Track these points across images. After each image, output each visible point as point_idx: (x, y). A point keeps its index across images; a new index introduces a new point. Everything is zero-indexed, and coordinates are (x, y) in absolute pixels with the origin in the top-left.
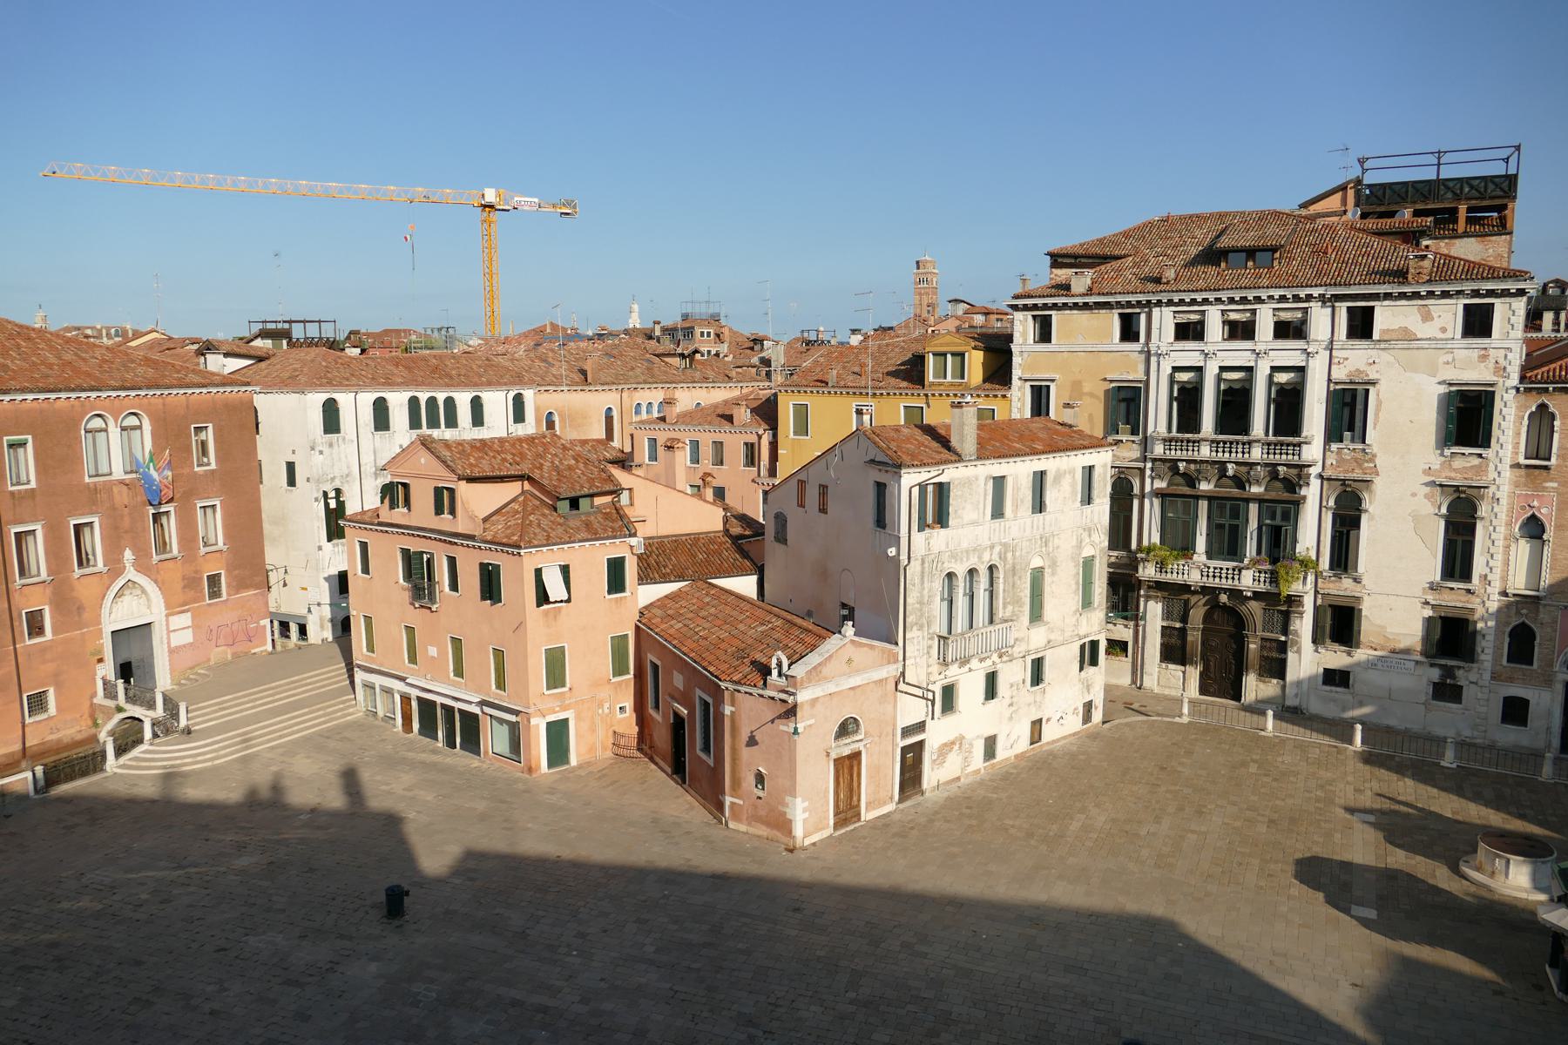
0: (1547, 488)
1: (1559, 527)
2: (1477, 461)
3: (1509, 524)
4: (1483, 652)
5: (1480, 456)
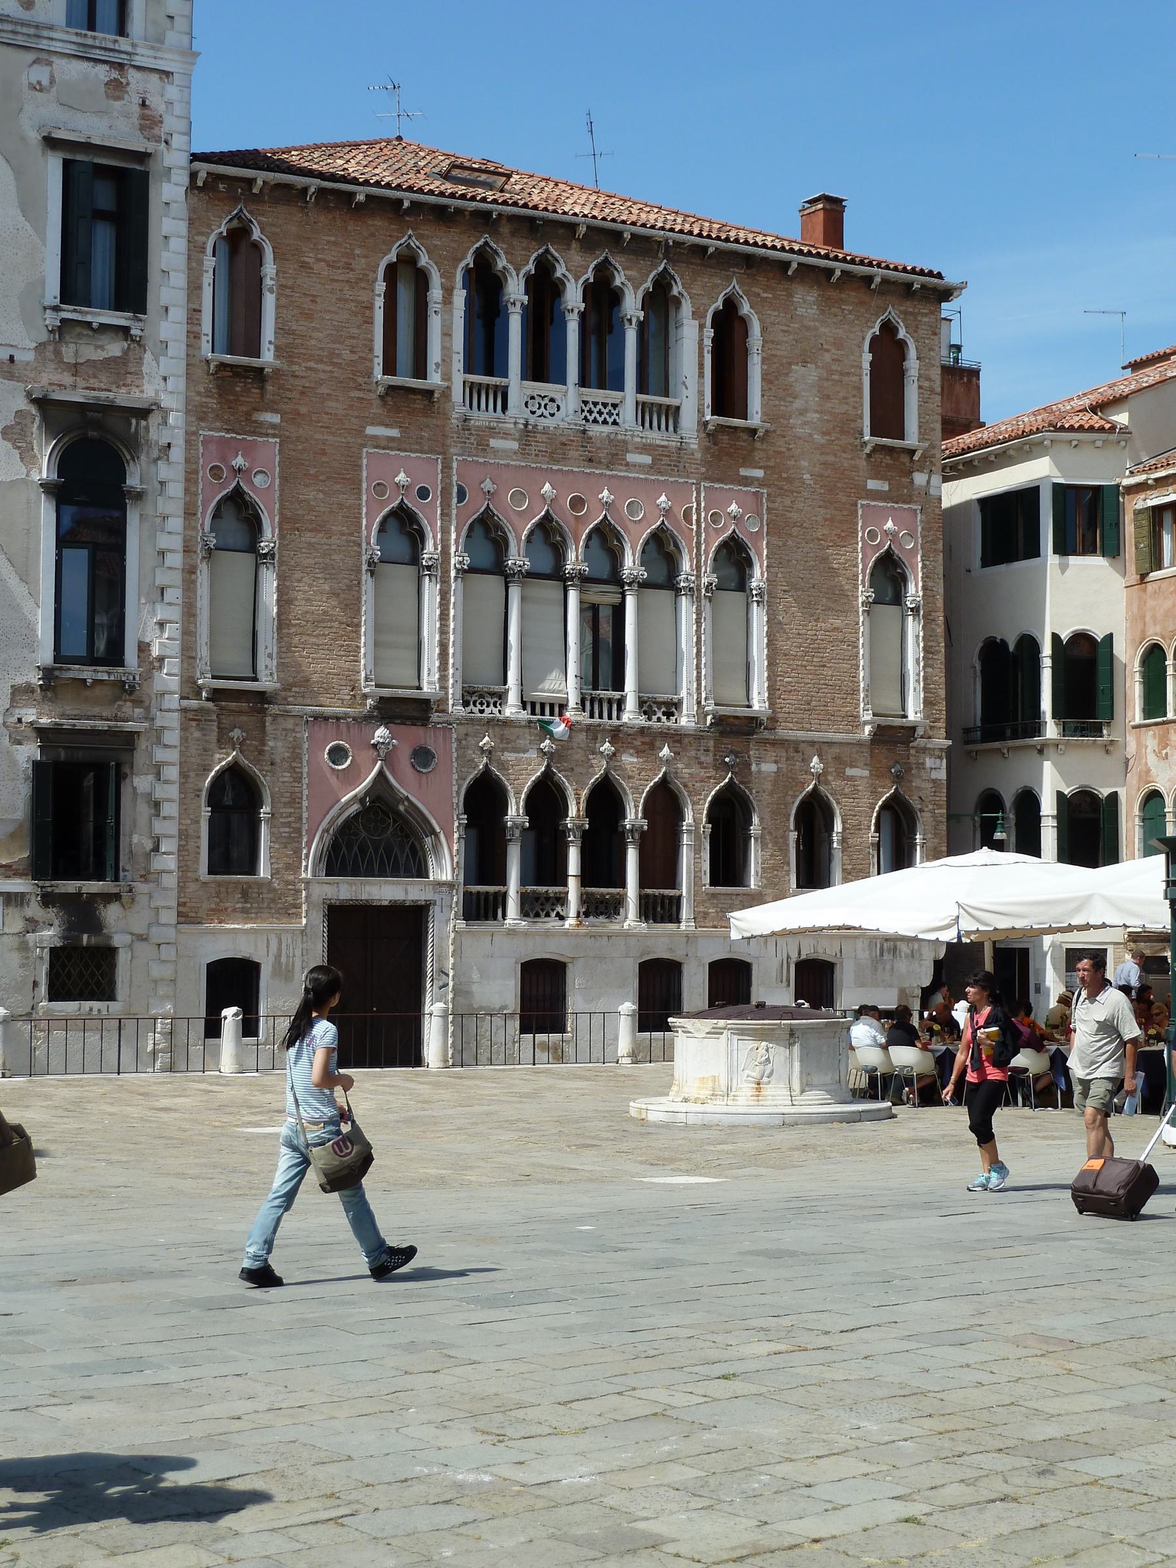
1: (288, 524)
2: (115, 348)
3: (189, 513)
4: (156, 849)
5: (125, 330)
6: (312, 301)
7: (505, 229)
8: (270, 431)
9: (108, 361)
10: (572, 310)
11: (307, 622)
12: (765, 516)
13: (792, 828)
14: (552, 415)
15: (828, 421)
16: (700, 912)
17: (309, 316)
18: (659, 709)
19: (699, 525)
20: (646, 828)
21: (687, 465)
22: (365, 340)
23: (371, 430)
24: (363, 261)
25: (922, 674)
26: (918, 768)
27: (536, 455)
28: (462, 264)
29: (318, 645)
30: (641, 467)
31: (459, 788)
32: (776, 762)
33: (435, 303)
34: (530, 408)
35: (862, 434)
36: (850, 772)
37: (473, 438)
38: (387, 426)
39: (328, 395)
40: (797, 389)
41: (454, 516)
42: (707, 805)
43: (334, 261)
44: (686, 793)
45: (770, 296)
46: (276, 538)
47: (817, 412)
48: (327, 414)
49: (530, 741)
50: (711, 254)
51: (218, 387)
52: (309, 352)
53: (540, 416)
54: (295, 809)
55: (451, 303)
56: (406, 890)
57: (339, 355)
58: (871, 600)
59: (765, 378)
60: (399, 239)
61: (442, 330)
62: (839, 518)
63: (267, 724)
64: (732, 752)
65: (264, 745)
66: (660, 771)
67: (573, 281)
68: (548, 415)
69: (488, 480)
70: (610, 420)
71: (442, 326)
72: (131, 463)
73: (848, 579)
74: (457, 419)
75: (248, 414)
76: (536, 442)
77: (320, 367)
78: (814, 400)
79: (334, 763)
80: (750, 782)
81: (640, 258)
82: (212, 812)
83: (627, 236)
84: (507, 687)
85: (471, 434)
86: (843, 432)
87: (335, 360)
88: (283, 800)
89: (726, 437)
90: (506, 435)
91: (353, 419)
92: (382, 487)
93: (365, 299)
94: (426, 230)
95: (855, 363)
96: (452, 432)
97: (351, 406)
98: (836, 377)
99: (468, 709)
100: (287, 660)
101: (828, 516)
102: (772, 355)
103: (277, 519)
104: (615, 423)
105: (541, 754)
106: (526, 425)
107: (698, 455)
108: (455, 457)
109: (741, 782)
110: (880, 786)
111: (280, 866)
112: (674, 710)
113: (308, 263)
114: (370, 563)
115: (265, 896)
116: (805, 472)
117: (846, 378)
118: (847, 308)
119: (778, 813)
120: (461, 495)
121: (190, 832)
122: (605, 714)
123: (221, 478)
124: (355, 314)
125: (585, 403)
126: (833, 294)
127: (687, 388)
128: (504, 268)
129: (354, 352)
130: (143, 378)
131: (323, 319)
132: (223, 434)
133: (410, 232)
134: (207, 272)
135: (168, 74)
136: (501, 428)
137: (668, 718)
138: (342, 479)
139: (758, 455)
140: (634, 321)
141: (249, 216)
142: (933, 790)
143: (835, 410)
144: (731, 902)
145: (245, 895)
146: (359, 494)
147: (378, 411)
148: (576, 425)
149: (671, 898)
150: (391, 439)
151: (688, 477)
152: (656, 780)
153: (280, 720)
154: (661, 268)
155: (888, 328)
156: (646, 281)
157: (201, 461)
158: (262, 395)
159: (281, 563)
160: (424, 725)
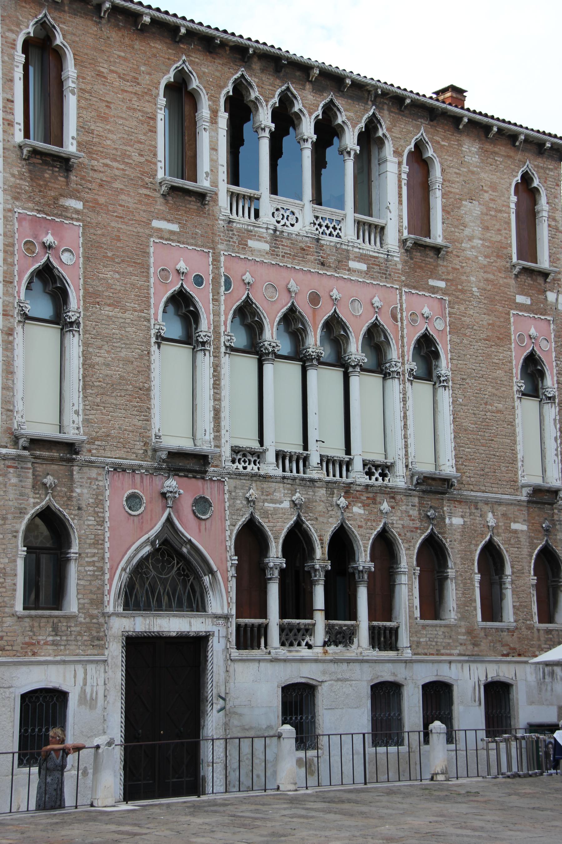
0: (66, 209)
6: (107, 106)
7: (257, 65)
8: (75, 216)
10: (307, 140)
11: (108, 384)
12: (448, 319)
13: (476, 571)
14: (292, 225)
15: (489, 247)
16: (413, 641)
17: (104, 119)
18: (376, 470)
19: (402, 323)
20: (373, 569)
22: (150, 146)
23: (156, 224)
24: (147, 77)
28: (224, 92)
29: (116, 405)
30: (360, 272)
31: (231, 533)
32: (462, 517)
33: (204, 121)
34: (276, 218)
35: (511, 258)
36: (514, 526)
37: (235, 238)
38: (169, 221)
39: (121, 189)
40: (467, 220)
41: (222, 302)
42: (416, 551)
43: (124, 74)
44: (400, 541)
45: (447, 144)
46: (81, 310)
47: (480, 239)
48: (121, 205)
49: (284, 494)
50: (408, 104)
51: (30, 171)
52: (105, 150)
53: (284, 225)
54: (98, 549)
55: (216, 123)
56: (190, 623)
57: (129, 157)
58: (522, 389)
59: (444, 210)
60: (175, 62)
61: (210, 145)
62: (498, 324)
63: (75, 473)
64: (431, 507)
65: (72, 491)
67: (307, 116)
68: (289, 225)
69: (248, 273)
70: (335, 233)
71: (210, 141)
73: (506, 372)
74: (223, 220)
75: (56, 199)
76: (283, 245)
77: (115, 164)
78: (478, 231)
79: (130, 508)
80: (444, 533)
81: (356, 103)
83: (348, 81)
84: (264, 448)
85: (233, 234)
86: (498, 256)
87: (126, 160)
88: (88, 541)
89: (419, 254)
90: (260, 238)
91: (142, 212)
93: (149, 111)
94: (197, 57)
95: (505, 203)
96: (219, 232)
97: (140, 202)
98: (493, 213)
99: (235, 466)
100: (91, 417)
101: (491, 322)
102: (449, 191)
103: (81, 292)
104: (338, 236)
105: (292, 505)
106: (275, 230)
107: (400, 266)
108: (222, 252)
109: (439, 533)
110: (535, 538)
111: (86, 601)
112: (387, 472)
113: (103, 73)
115: (73, 629)
116: (474, 286)
117: (499, 214)
118: (499, 159)
119: (466, 558)
121: (8, 569)
122: (331, 474)
123: (34, 252)
125: (317, 218)
126: (488, 147)
127: (390, 212)
128: (256, 98)
131: (116, 123)
132: (35, 214)
133: (184, 57)
134: (18, 67)
136: (256, 232)
137: (383, 480)
138: (134, 263)
139: (441, 270)
140: (352, 153)
141: (53, 22)
143: (492, 239)
144: (436, 632)
145: (56, 630)
146: (148, 277)
147: (161, 208)
148: (312, 233)
149: (391, 629)
150: (172, 232)
151: (393, 283)
152: (379, 529)
153: (85, 469)
154: (371, 113)
155: (526, 178)
156: (360, 122)
157: (17, 235)
158: (67, 185)
159: (85, 332)
160: (203, 478)
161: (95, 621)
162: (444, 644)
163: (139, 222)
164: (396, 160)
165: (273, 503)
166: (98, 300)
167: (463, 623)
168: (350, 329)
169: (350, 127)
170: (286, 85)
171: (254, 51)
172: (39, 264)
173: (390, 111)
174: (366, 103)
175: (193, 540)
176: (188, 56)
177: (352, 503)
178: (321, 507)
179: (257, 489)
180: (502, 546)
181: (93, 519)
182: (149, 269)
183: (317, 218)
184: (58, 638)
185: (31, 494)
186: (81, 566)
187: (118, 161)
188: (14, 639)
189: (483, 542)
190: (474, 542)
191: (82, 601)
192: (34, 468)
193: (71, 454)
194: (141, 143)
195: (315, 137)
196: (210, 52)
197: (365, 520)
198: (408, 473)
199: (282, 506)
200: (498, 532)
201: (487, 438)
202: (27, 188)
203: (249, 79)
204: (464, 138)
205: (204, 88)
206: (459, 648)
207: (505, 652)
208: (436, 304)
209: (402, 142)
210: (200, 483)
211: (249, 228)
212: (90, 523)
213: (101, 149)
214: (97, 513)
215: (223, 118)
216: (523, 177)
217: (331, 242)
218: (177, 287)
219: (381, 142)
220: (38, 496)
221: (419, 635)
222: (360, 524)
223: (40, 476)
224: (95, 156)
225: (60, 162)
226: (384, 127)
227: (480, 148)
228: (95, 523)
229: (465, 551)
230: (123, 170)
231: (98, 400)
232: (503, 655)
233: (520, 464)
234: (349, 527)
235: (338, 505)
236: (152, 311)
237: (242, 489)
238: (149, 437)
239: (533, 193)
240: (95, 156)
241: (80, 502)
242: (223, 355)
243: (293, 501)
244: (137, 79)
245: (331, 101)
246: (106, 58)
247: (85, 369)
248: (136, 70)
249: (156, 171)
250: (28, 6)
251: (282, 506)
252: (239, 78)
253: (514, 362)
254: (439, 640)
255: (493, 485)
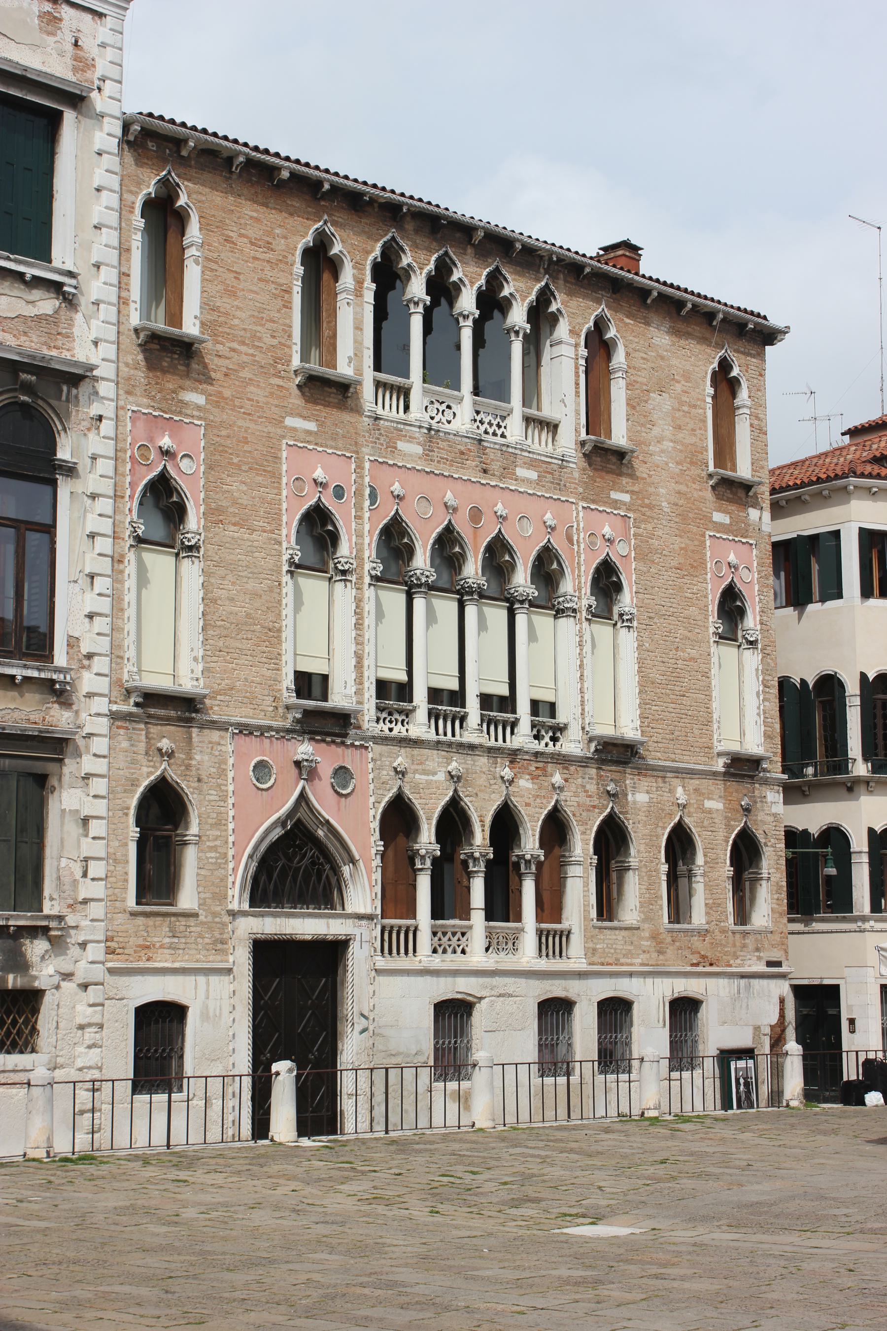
0: (186, 404)
1: (214, 515)
2: (47, 304)
4: (85, 875)
6: (235, 278)
7: (410, 226)
8: (195, 413)
9: (39, 318)
10: (468, 316)
11: (232, 623)
12: (633, 542)
13: (663, 860)
15: (681, 451)
17: (231, 293)
18: (547, 733)
19: (579, 546)
21: (568, 484)
22: (285, 325)
23: (290, 422)
24: (283, 241)
25: (762, 707)
26: (761, 801)
27: (438, 462)
28: (371, 258)
36: (708, 804)
37: (382, 438)
38: (305, 418)
39: (250, 379)
41: (366, 520)
42: (593, 835)
43: (256, 239)
44: (575, 823)
47: (672, 441)
48: (249, 399)
50: (588, 273)
51: (146, 359)
52: (233, 331)
53: (438, 422)
54: (221, 831)
55: (361, 296)
57: (260, 339)
58: (720, 631)
61: (354, 323)
62: (692, 548)
66: (552, 798)
67: (469, 287)
68: (445, 422)
69: (397, 483)
70: (499, 432)
71: (355, 318)
72: (62, 433)
73: (700, 609)
74: (369, 417)
76: (438, 448)
77: (243, 349)
78: (668, 432)
79: (258, 780)
80: (626, 813)
81: (526, 271)
82: (140, 833)
83: (518, 246)
84: (414, 704)
85: (380, 434)
86: (692, 463)
87: (256, 343)
88: (210, 821)
89: (599, 459)
90: (411, 439)
91: (273, 408)
92: (300, 482)
94: (340, 217)
95: (700, 397)
97: (272, 394)
98: (686, 408)
101: (683, 545)
102: (635, 381)
107: (576, 475)
108: (367, 457)
111: (208, 895)
113: (232, 237)
114: (291, 563)
115: (192, 929)
116: (663, 499)
119: (652, 845)
120: (373, 497)
123: (148, 459)
124: (275, 296)
126: (680, 326)
127: (566, 406)
128: (409, 265)
129: (274, 337)
130: (74, 340)
133: (326, 217)
135: (101, 15)
136: (407, 431)
137: (554, 746)
138: (264, 471)
141: (177, 180)
142: (774, 824)
143: (685, 441)
144: (614, 937)
146: (279, 488)
150: (309, 432)
152: (550, 808)
155: (725, 366)
161: (217, 920)
162: (624, 952)
163: (270, 420)
164: (573, 341)
165: (424, 774)
166: (221, 518)
167: (646, 926)
168: (518, 554)
169: (519, 300)
170: (444, 249)
171: (408, 209)
172: (155, 473)
173: (566, 281)
174: (538, 271)
175: (332, 821)
176: (329, 215)
177: (519, 775)
178: (482, 781)
179: (407, 757)
180: (693, 830)
181: (215, 793)
182: (280, 479)
183: (478, 413)
184: (176, 940)
185: (145, 762)
186: (202, 851)
187: (248, 345)
188: (126, 940)
189: (672, 825)
190: (660, 824)
191: (203, 895)
192: (147, 729)
193: (191, 712)
194: (274, 322)
195: (477, 313)
196: (356, 211)
197: (533, 796)
198: (585, 737)
199: (435, 778)
200: (689, 812)
201: (678, 693)
202: (142, 380)
203: (401, 242)
204: (653, 315)
205: (349, 253)
206: (641, 956)
207: (695, 961)
208: (619, 521)
209: (580, 320)
210: (340, 750)
211: (399, 426)
212: (212, 798)
213: (228, 330)
214: (219, 786)
215: (370, 288)
216: (720, 364)
217: (495, 443)
218: (313, 501)
219: (554, 319)
220: (152, 764)
221: (595, 941)
222: (527, 801)
223: (154, 739)
224: (220, 339)
225: (180, 347)
226: (559, 301)
227: (670, 327)
228: (217, 798)
229: (651, 836)
230: (253, 355)
231: (221, 644)
232: (693, 965)
233: (715, 726)
234: (515, 806)
235: (502, 778)
236: (284, 532)
237: (388, 756)
238: (280, 690)
239: (733, 385)
240: (220, 339)
241: (200, 772)
242: (366, 586)
243: (449, 772)
244: (271, 244)
245: (497, 269)
246: (235, 219)
247: (206, 605)
248: (269, 233)
249: (291, 356)
250: (150, 163)
251: (435, 778)
252: (389, 241)
253: (710, 597)
254: (618, 947)
255: (684, 753)
